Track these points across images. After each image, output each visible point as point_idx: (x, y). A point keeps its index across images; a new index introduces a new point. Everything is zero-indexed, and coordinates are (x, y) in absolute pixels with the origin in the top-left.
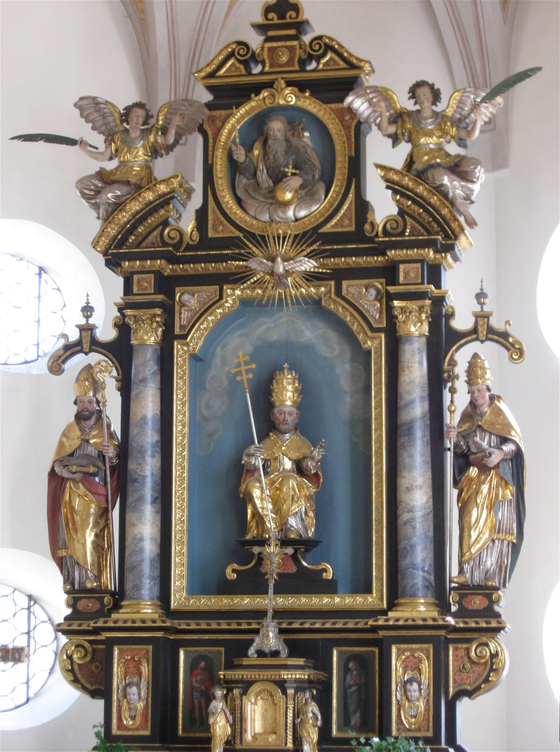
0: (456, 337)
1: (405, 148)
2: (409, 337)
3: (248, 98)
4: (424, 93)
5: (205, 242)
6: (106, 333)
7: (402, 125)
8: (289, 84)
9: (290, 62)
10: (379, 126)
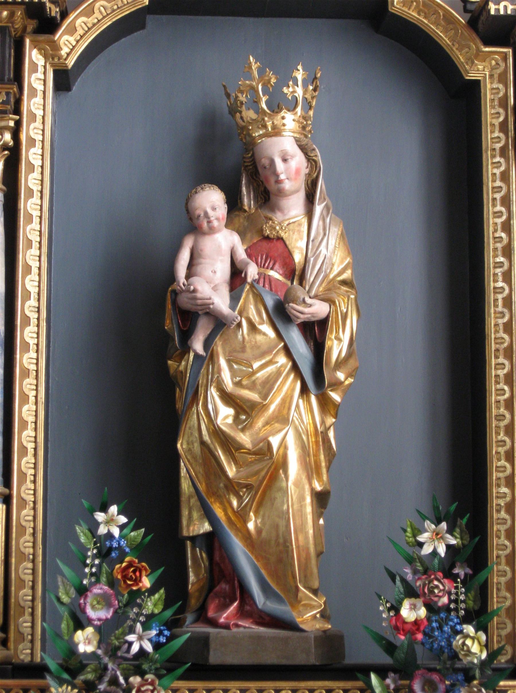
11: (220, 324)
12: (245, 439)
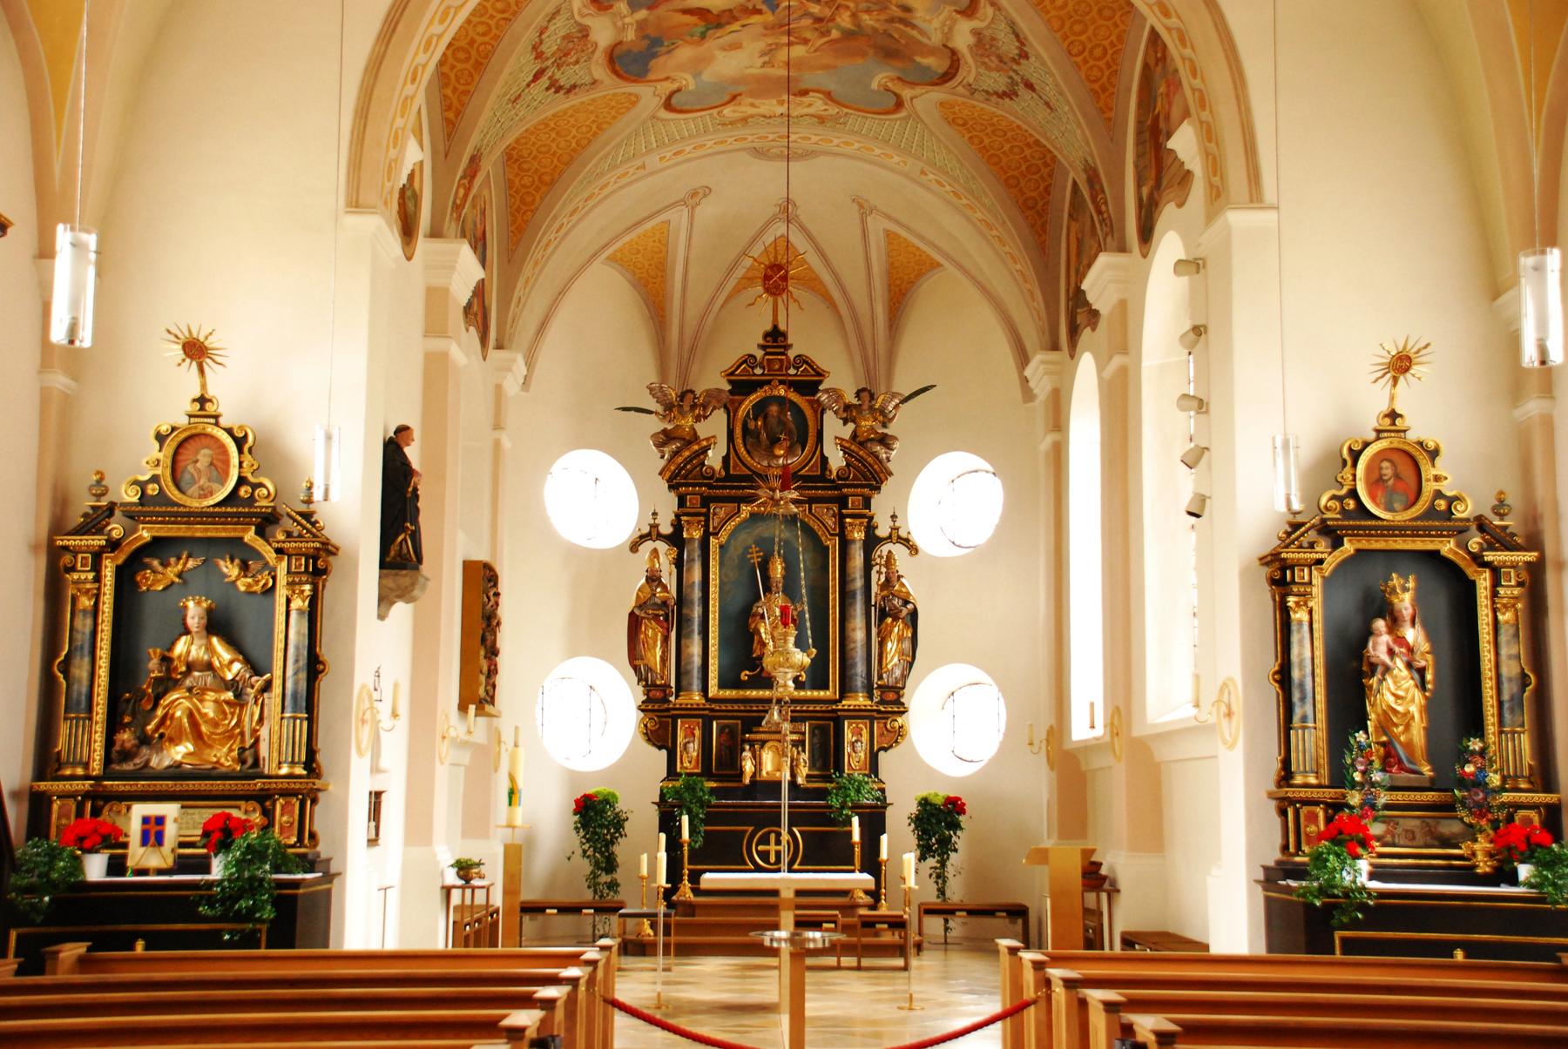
0: (880, 541)
1: (851, 426)
2: (853, 541)
3: (755, 391)
4: (865, 395)
5: (729, 477)
6: (666, 529)
7: (849, 413)
8: (781, 382)
9: (780, 369)
10: (836, 412)
11: (1387, 669)
12: (1400, 709)
